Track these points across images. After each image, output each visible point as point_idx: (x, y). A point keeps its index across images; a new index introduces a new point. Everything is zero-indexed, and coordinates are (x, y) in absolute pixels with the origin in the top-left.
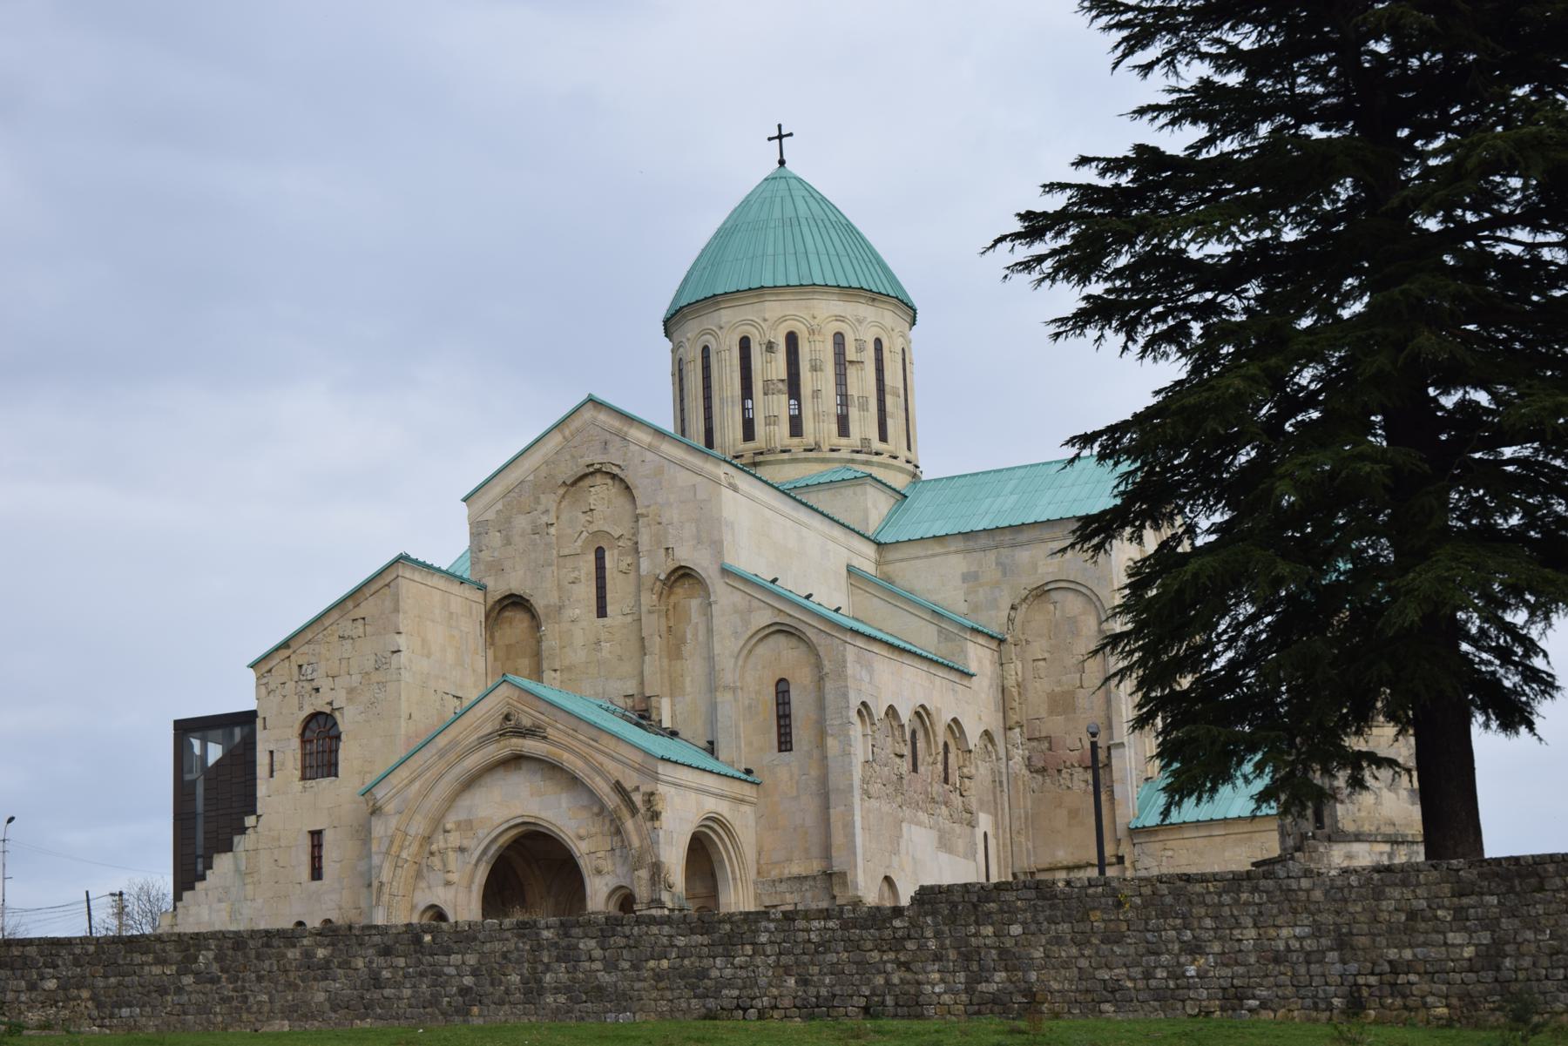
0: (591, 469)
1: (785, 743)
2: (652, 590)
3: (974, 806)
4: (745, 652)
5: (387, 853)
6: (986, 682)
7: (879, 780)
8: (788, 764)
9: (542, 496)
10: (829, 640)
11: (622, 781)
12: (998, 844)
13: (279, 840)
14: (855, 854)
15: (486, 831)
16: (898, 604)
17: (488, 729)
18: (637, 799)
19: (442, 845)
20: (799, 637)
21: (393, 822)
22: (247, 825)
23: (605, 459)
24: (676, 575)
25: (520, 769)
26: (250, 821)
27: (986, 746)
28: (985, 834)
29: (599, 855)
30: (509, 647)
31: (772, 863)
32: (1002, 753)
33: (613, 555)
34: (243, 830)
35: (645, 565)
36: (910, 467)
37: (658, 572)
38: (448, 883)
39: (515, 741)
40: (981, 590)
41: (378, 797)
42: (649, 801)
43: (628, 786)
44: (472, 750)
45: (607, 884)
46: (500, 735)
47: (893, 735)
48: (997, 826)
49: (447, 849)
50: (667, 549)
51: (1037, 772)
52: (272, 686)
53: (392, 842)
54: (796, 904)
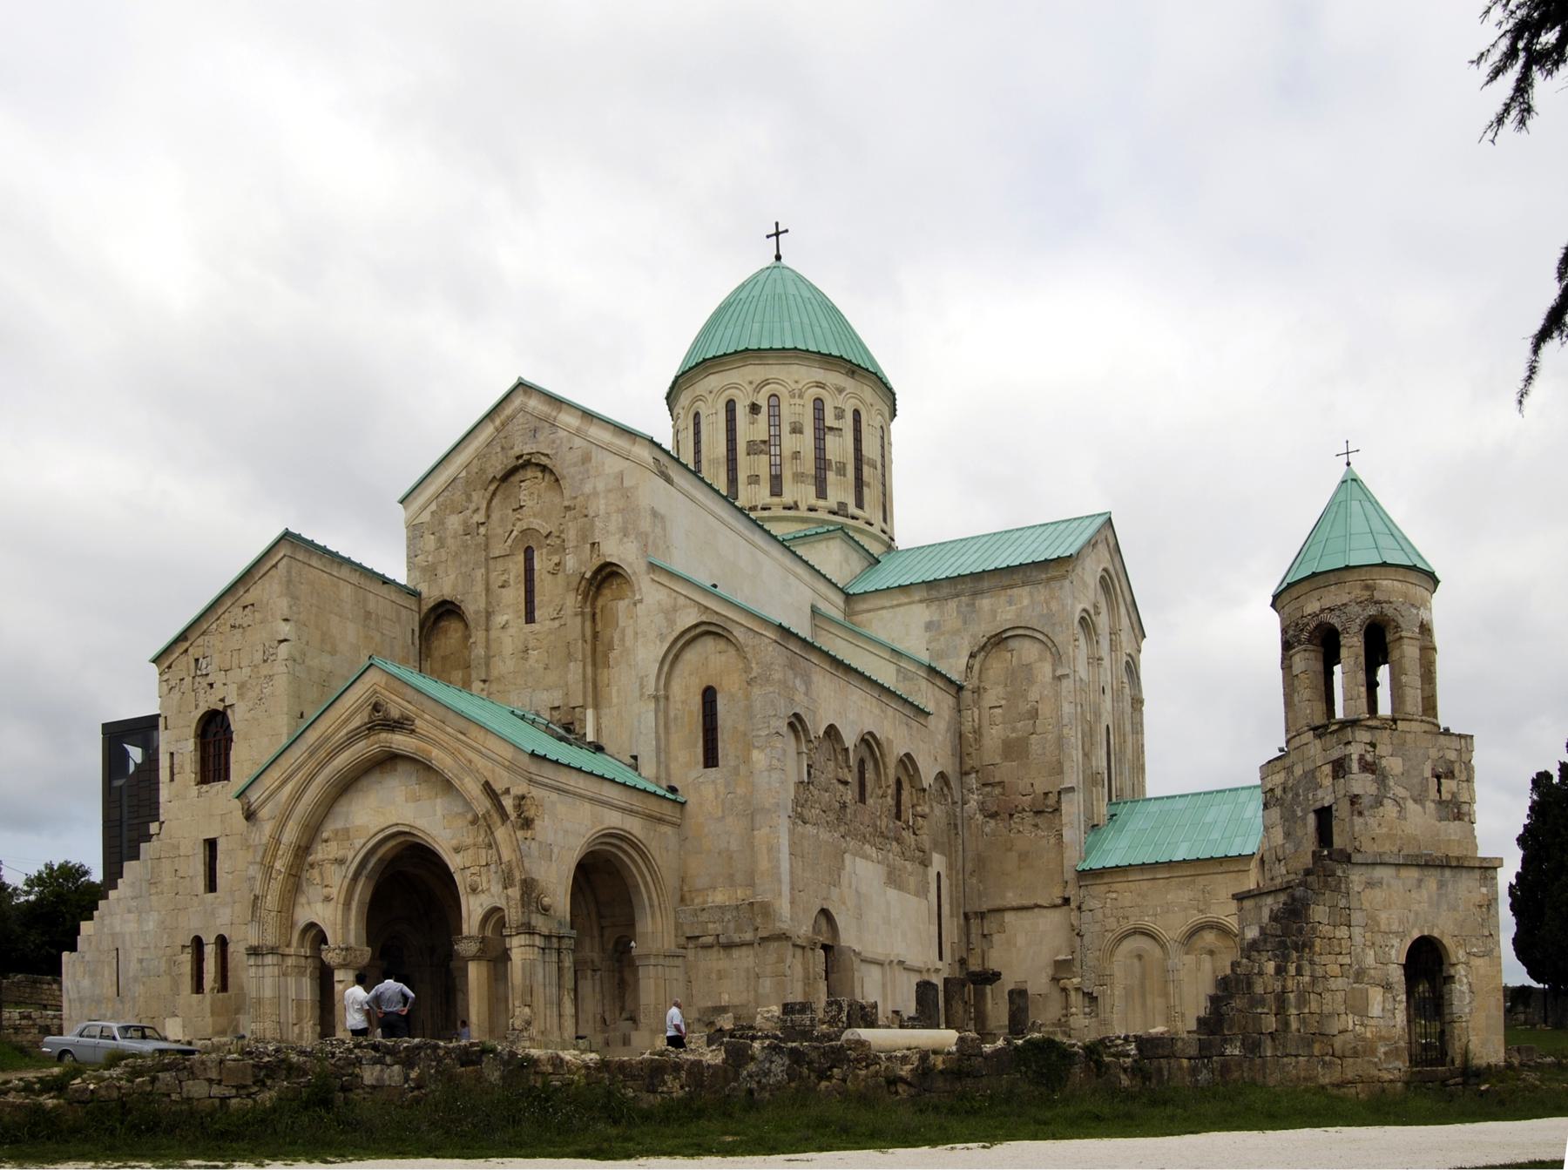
1: (711, 759)
2: (578, 590)
3: (927, 847)
6: (943, 726)
7: (817, 805)
8: (713, 782)
10: (757, 641)
11: (491, 782)
12: (951, 885)
14: (780, 881)
16: (859, 644)
17: (356, 722)
18: (508, 803)
20: (727, 639)
25: (395, 770)
27: (942, 789)
28: (939, 874)
29: (472, 870)
32: (957, 797)
35: (571, 562)
36: (885, 537)
39: (383, 735)
40: (942, 639)
42: (520, 805)
43: (498, 787)
46: (369, 729)
47: (836, 759)
48: (950, 867)
51: (993, 815)
54: (718, 936)
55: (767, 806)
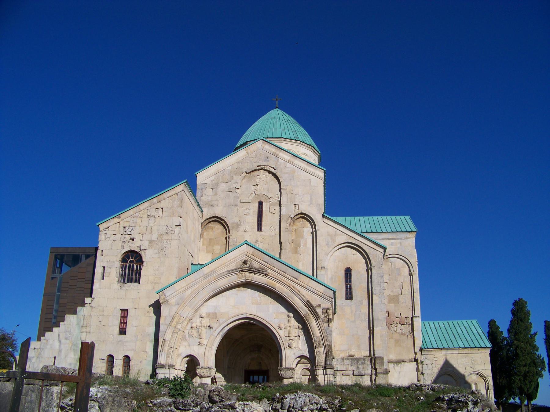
0: (259, 168)
1: (349, 296)
4: (331, 253)
5: (170, 324)
9: (234, 177)
11: (310, 301)
13: (103, 311)
15: (224, 319)
17: (233, 266)
18: (319, 311)
19: (198, 324)
21: (174, 309)
22: (86, 302)
23: (266, 164)
24: (298, 216)
26: (88, 300)
30: (210, 240)
31: (341, 351)
33: (267, 205)
34: (83, 304)
37: (290, 214)
38: (200, 344)
39: (248, 274)
41: (167, 295)
42: (327, 312)
43: (314, 303)
44: (221, 276)
45: (294, 354)
49: (201, 326)
50: (295, 205)
52: (108, 235)
53: (173, 319)
55: (380, 318)
